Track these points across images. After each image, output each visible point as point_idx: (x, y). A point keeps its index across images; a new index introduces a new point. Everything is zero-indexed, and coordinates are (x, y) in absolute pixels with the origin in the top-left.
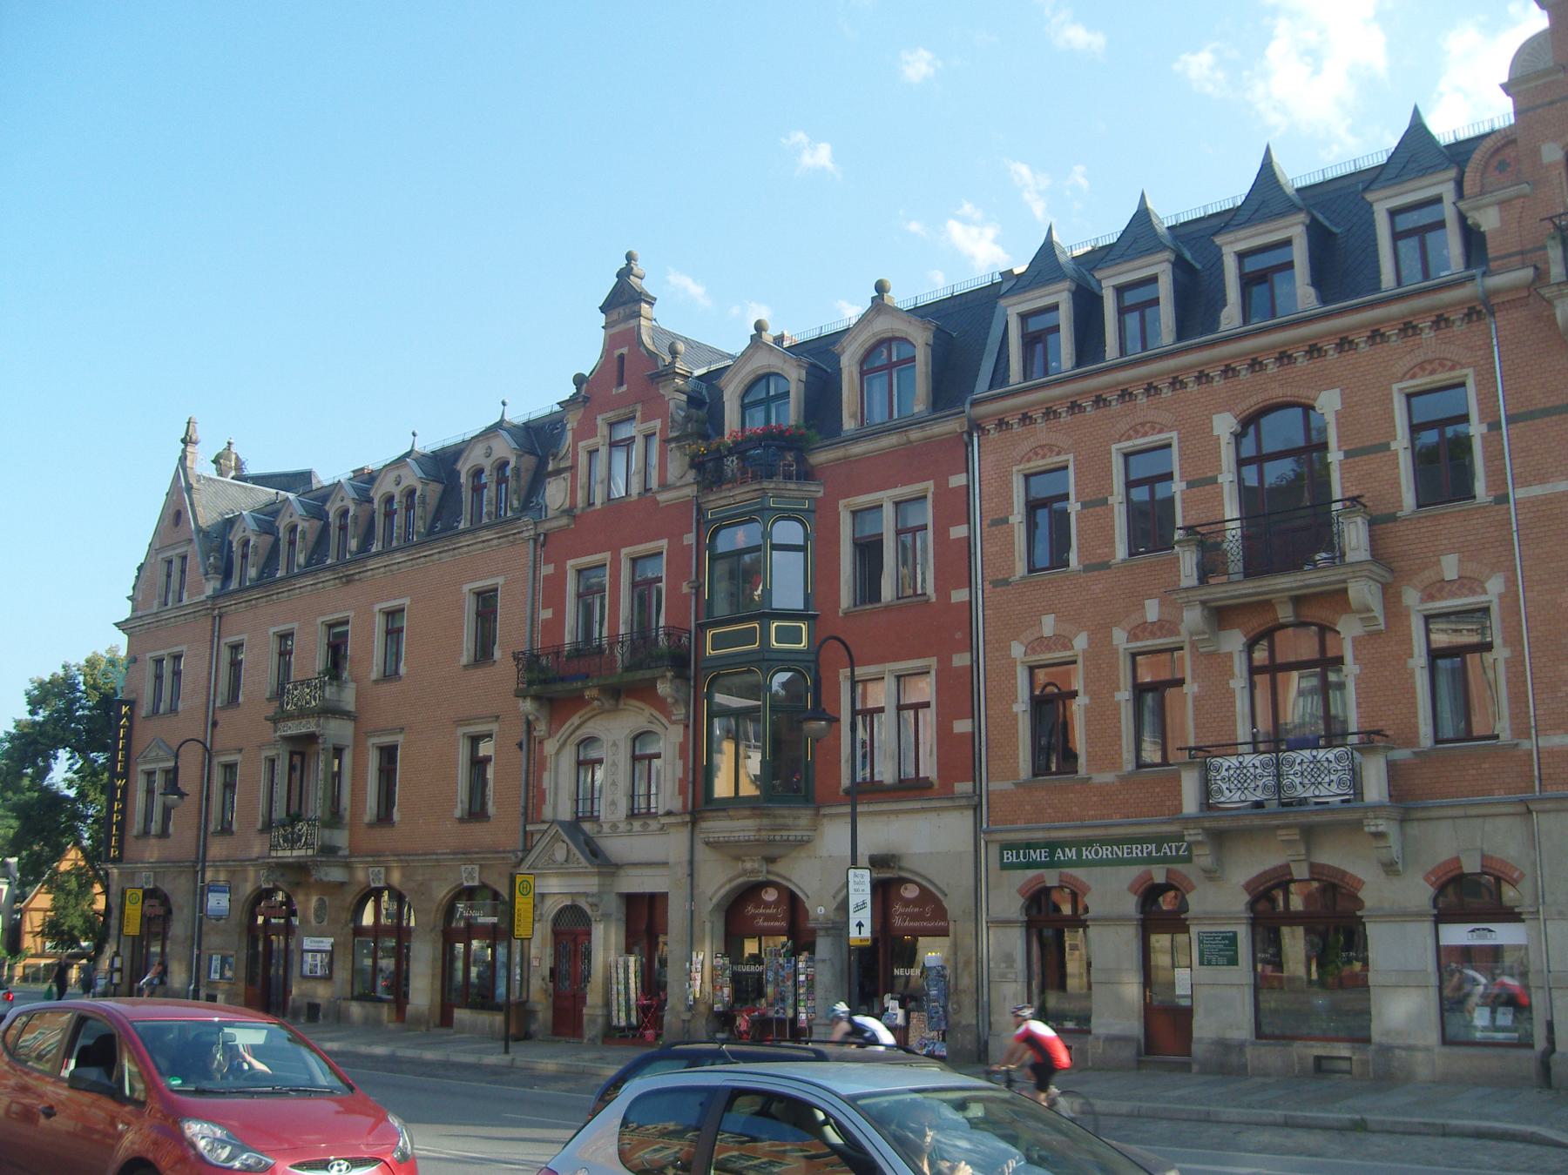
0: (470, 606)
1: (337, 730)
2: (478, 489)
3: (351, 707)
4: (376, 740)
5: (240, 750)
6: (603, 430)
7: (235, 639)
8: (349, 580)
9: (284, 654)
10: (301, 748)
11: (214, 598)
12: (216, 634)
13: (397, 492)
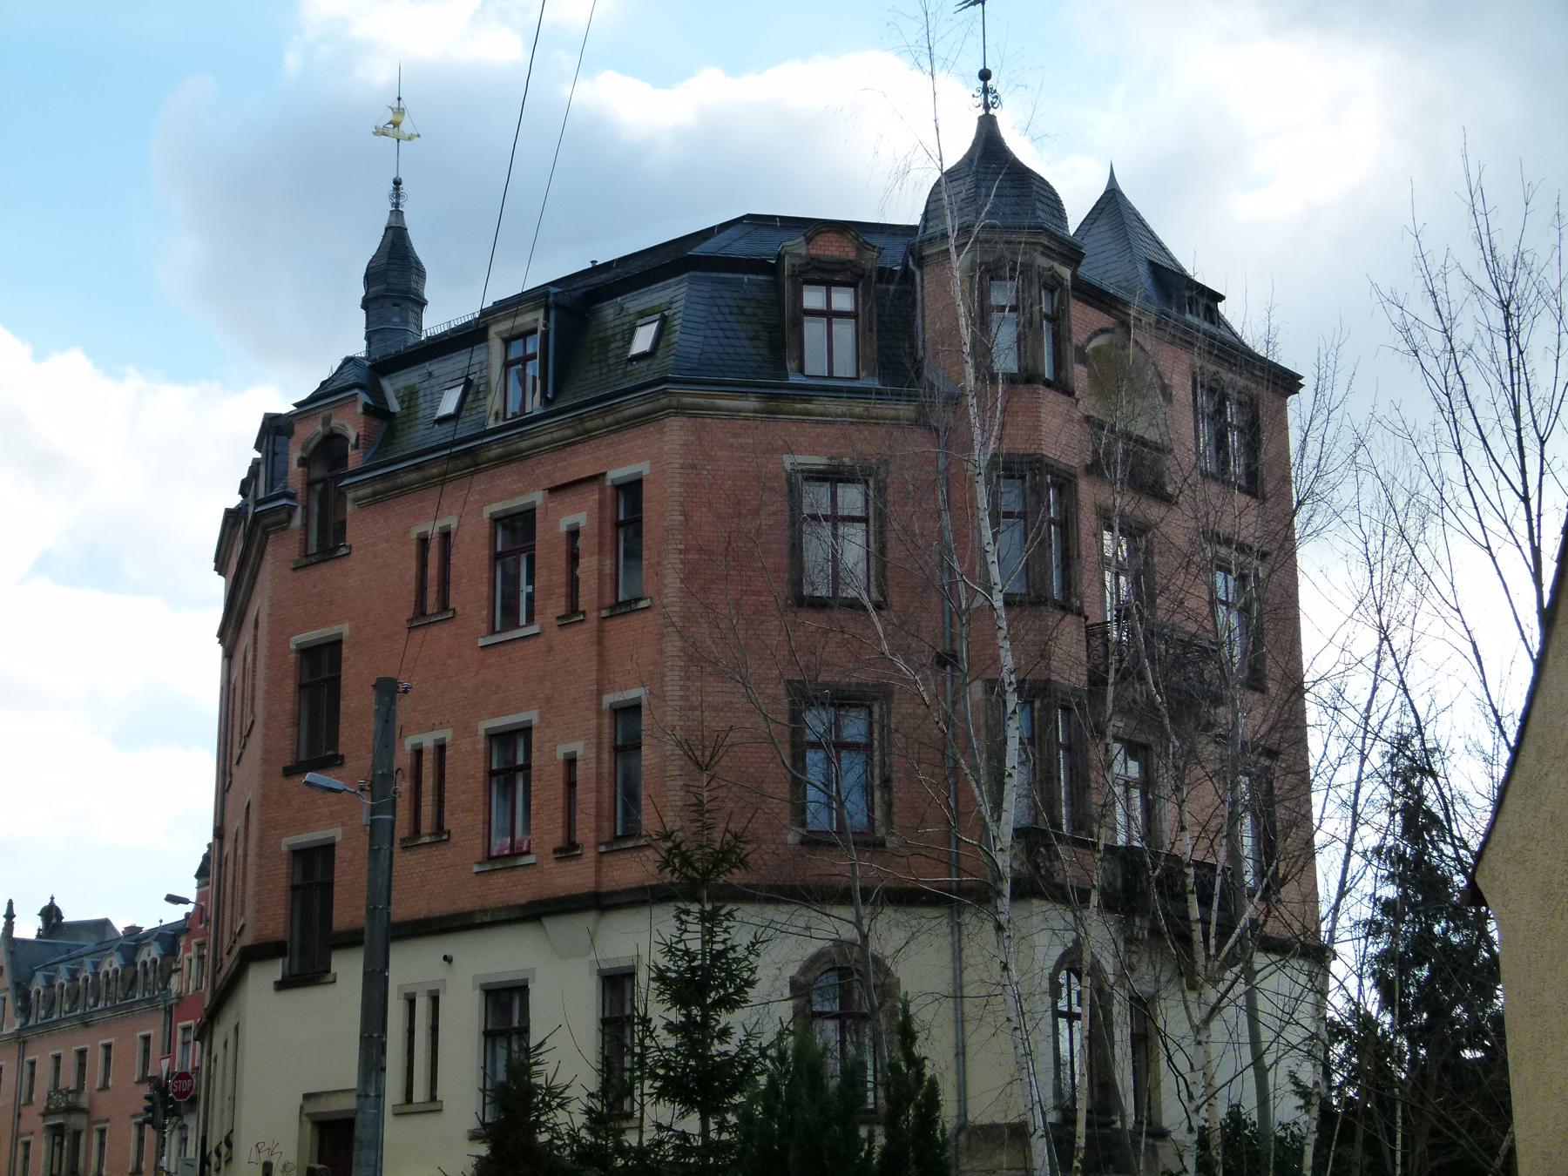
0: (140, 1045)
1: (76, 1121)
2: (146, 974)
3: (86, 1106)
4: (97, 1126)
5: (32, 1133)
6: (194, 948)
7: (31, 1058)
8: (86, 1025)
9: (57, 1069)
10: (57, 1131)
11: (19, 1030)
12: (22, 1055)
13: (110, 970)
